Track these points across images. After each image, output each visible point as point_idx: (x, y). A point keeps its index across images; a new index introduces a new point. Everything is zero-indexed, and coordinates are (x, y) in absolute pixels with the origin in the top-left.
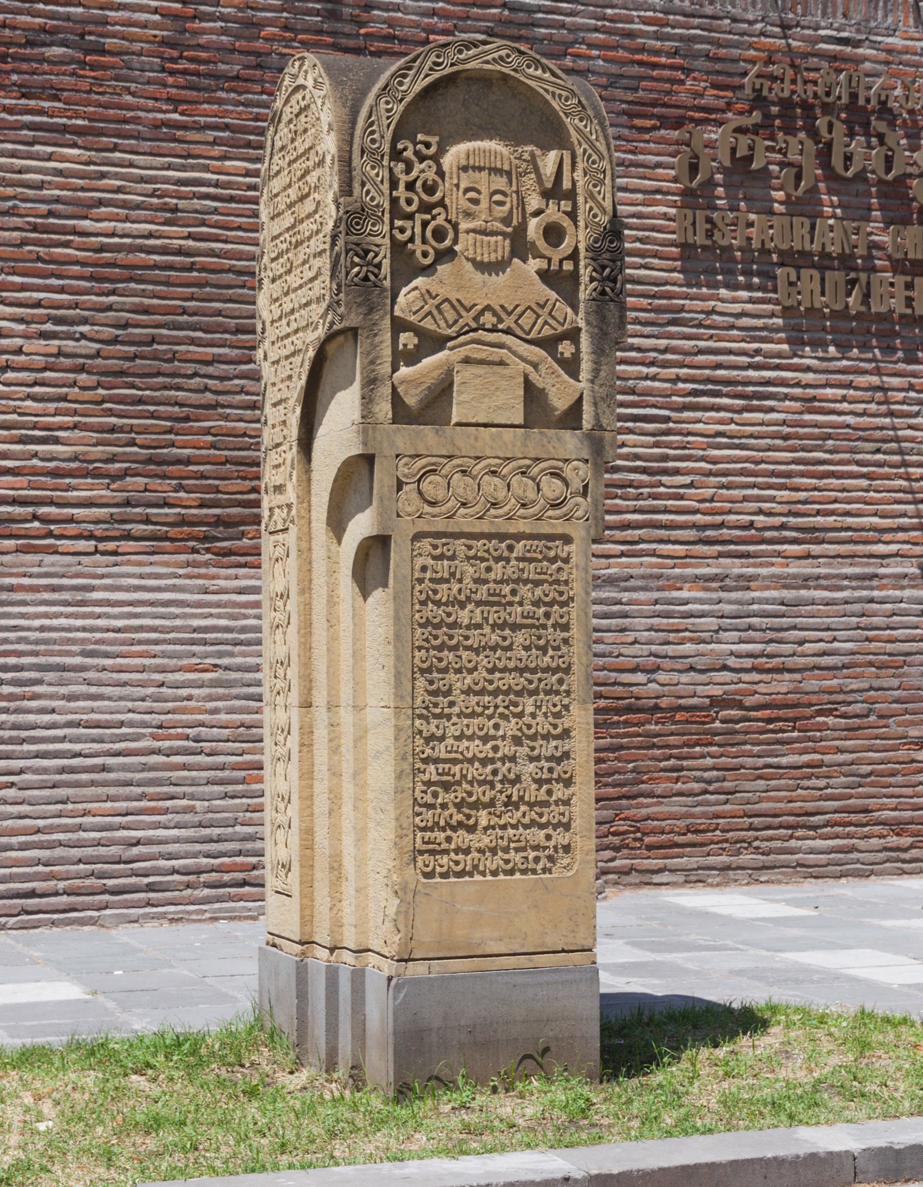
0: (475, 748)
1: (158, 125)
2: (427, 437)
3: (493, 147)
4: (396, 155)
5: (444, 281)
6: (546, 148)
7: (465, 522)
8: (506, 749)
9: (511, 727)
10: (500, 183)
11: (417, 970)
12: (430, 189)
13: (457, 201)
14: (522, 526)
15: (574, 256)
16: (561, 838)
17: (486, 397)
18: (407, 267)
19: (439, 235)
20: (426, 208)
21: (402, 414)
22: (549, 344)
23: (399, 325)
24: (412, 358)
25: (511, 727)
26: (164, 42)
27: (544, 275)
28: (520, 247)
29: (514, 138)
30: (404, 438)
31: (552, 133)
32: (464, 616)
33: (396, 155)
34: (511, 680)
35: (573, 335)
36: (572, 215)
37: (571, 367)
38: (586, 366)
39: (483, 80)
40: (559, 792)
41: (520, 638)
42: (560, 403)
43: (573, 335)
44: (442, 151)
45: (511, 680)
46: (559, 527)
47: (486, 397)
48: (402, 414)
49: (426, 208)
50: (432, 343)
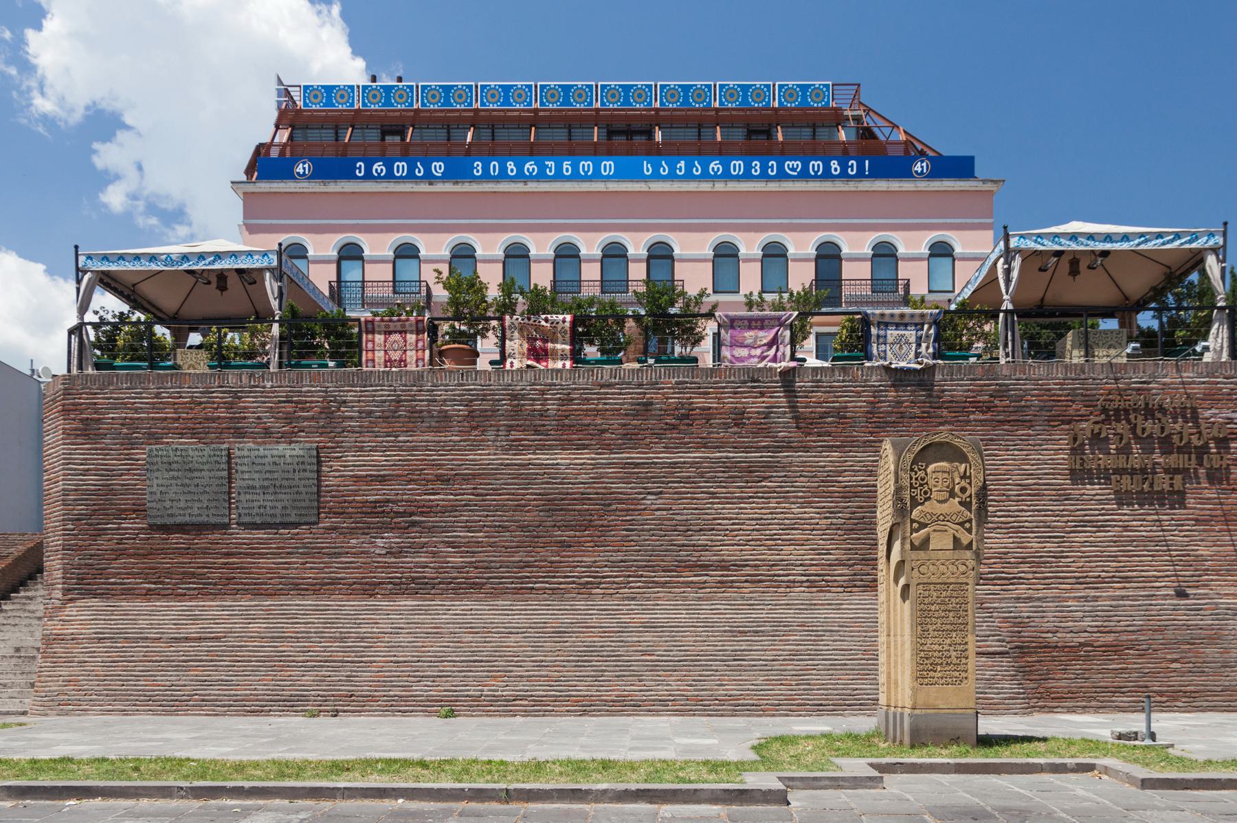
0: (936, 647)
1: (865, 442)
2: (922, 554)
3: (944, 464)
4: (912, 470)
5: (927, 507)
6: (961, 463)
7: (933, 579)
8: (946, 647)
9: (948, 641)
10: (946, 475)
11: (917, 712)
12: (923, 479)
13: (932, 482)
14: (952, 580)
15: (970, 496)
16: (964, 675)
17: (941, 541)
18: (915, 503)
19: (926, 493)
20: (921, 485)
21: (913, 548)
22: (961, 524)
23: (913, 521)
24: (917, 531)
25: (948, 641)
26: (868, 412)
27: (960, 503)
28: (952, 494)
29: (951, 461)
30: (914, 555)
31: (963, 458)
32: (933, 608)
33: (912, 470)
34: (948, 627)
35: (970, 521)
36: (970, 484)
37: (969, 531)
38: (974, 530)
39: (941, 444)
40: (964, 661)
41: (951, 614)
42: (965, 542)
43: (970, 521)
44: (927, 466)
45: (948, 627)
46: (965, 580)
47: (941, 541)
48: (913, 548)
49: (921, 485)
50: (923, 526)
